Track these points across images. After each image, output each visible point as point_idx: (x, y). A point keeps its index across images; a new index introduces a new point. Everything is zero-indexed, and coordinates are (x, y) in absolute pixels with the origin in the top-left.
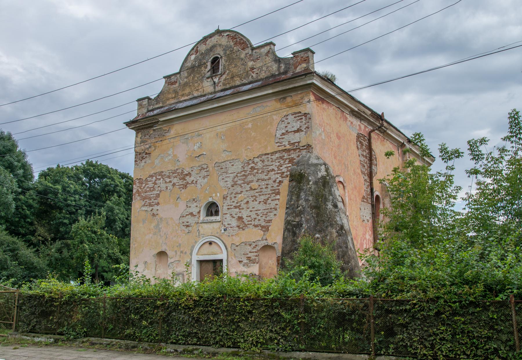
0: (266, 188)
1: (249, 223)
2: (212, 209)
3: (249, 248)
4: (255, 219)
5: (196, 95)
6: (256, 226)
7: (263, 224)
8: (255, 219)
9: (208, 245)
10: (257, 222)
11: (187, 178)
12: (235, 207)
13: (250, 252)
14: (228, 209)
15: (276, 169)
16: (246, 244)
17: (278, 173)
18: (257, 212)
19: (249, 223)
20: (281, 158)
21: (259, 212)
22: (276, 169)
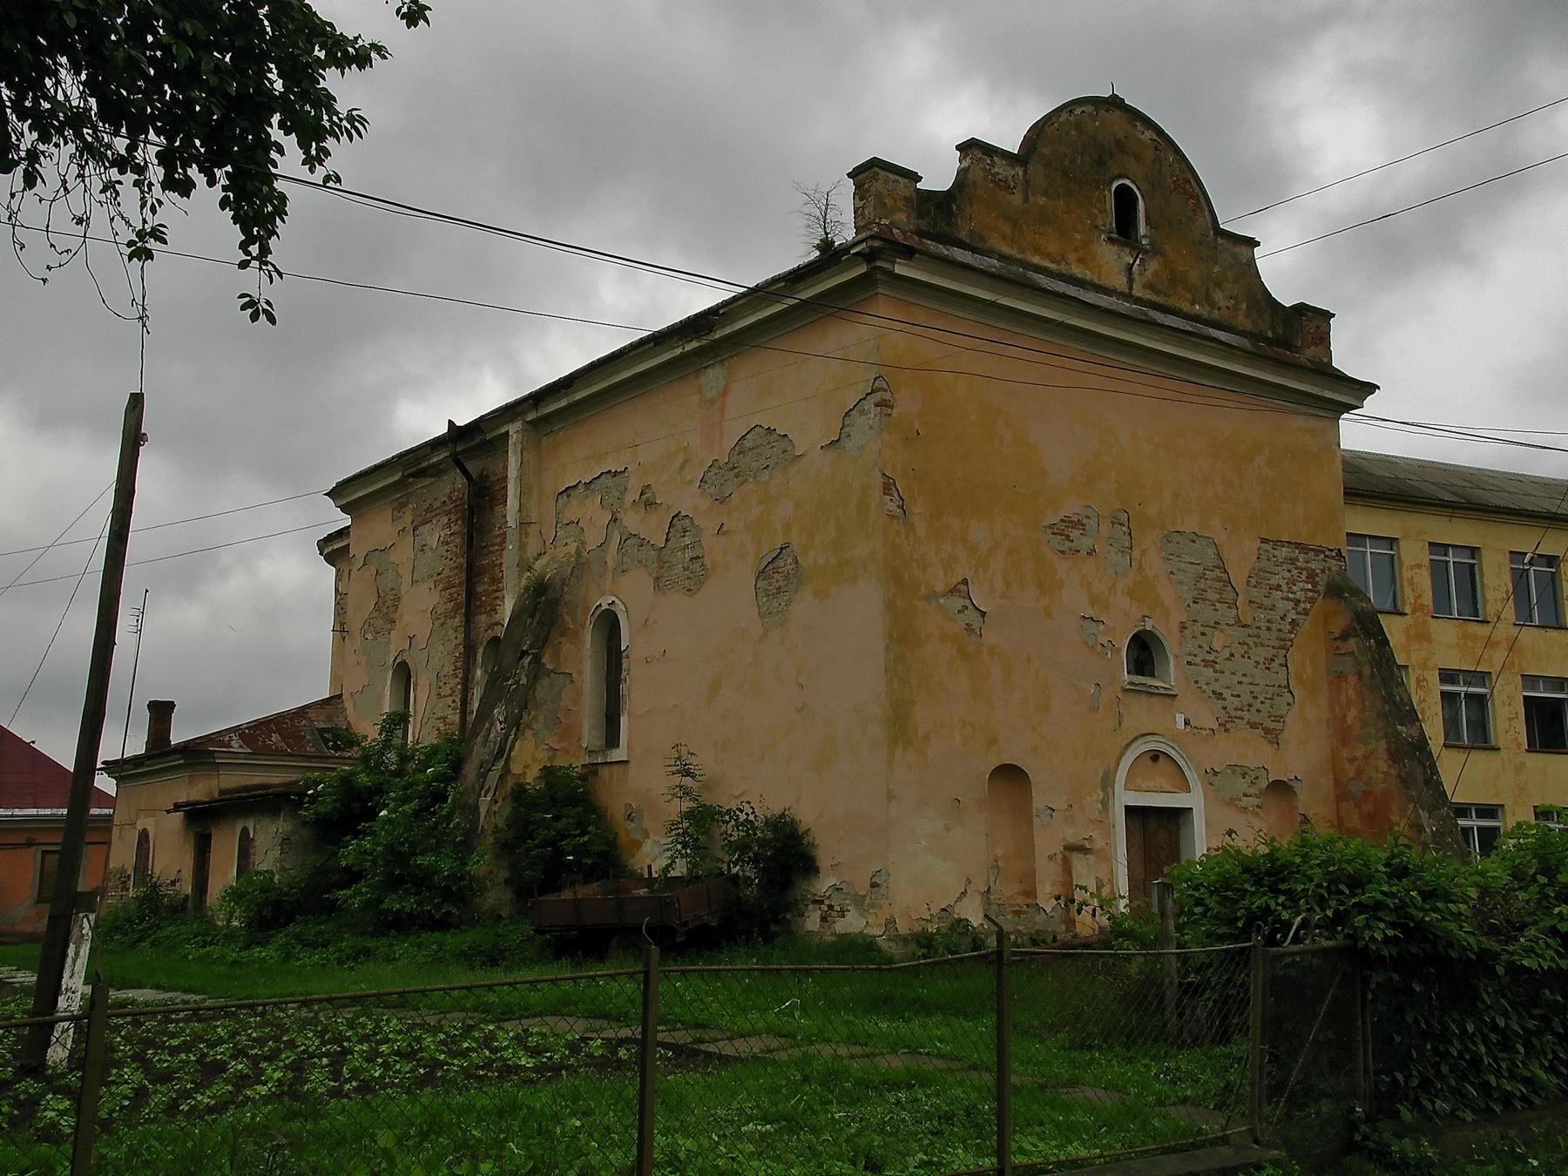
0: (1269, 629)
1: (1239, 713)
2: (1144, 653)
3: (1242, 785)
4: (1250, 705)
5: (1077, 270)
6: (1253, 726)
7: (1268, 723)
8: (1250, 705)
9: (1147, 760)
10: (1255, 718)
11: (1075, 534)
12: (1206, 663)
13: (1245, 795)
14: (1189, 663)
15: (1284, 587)
16: (1234, 772)
17: (1288, 599)
18: (1252, 688)
19: (1239, 713)
20: (1293, 561)
21: (1259, 689)
22: (1284, 587)
